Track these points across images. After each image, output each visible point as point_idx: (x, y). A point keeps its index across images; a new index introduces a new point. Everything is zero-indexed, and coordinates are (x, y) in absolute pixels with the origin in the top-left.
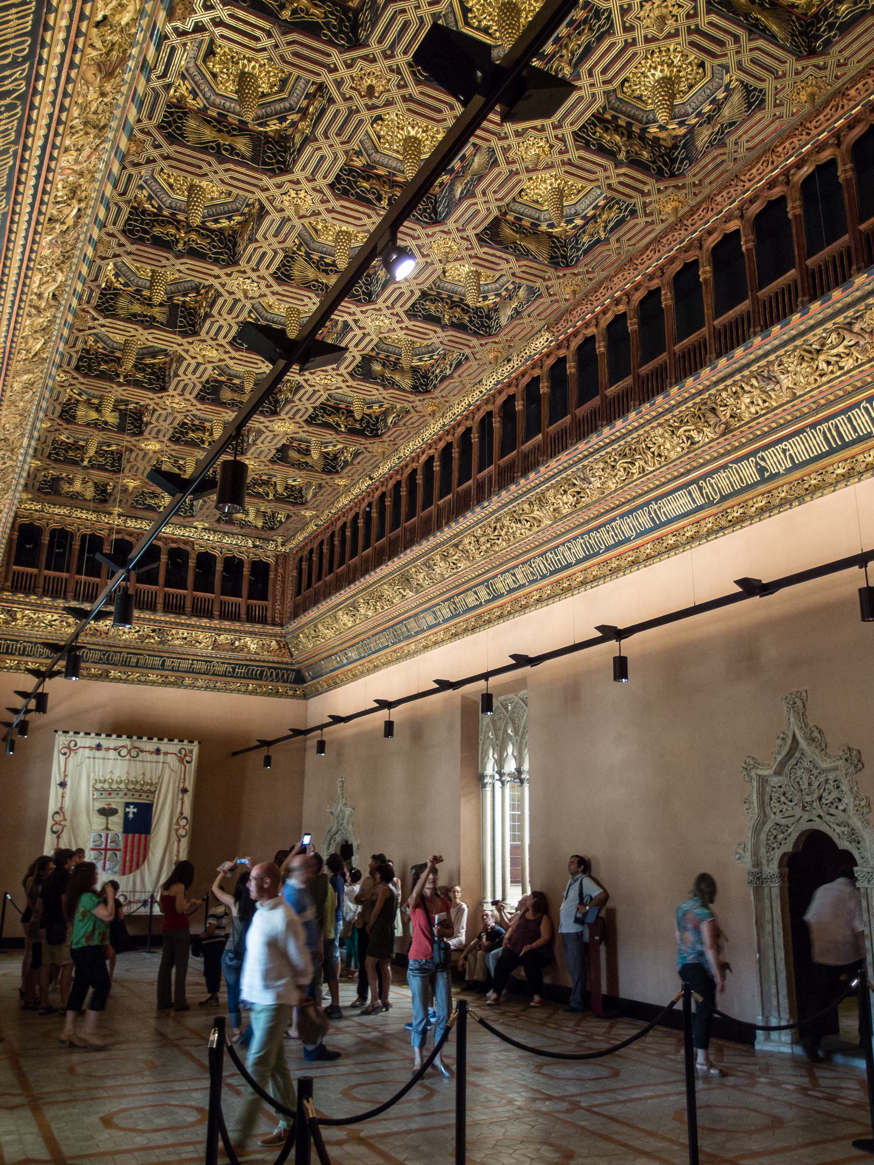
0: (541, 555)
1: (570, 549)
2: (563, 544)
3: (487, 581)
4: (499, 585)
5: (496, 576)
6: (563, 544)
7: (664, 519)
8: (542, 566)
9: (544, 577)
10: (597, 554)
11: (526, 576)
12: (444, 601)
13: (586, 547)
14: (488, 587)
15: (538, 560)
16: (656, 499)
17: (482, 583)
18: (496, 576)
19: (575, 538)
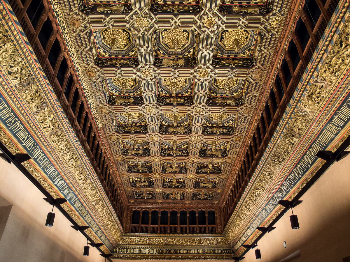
0: (56, 170)
1: (60, 180)
2: (61, 177)
3: (37, 144)
4: (37, 153)
5: (41, 149)
6: (61, 177)
7: (73, 204)
8: (51, 171)
9: (47, 174)
10: (60, 190)
11: (45, 165)
12: (13, 111)
13: (62, 186)
14: (34, 145)
15: (54, 168)
16: (78, 199)
17: (35, 142)
18: (41, 149)
19: (64, 181)
